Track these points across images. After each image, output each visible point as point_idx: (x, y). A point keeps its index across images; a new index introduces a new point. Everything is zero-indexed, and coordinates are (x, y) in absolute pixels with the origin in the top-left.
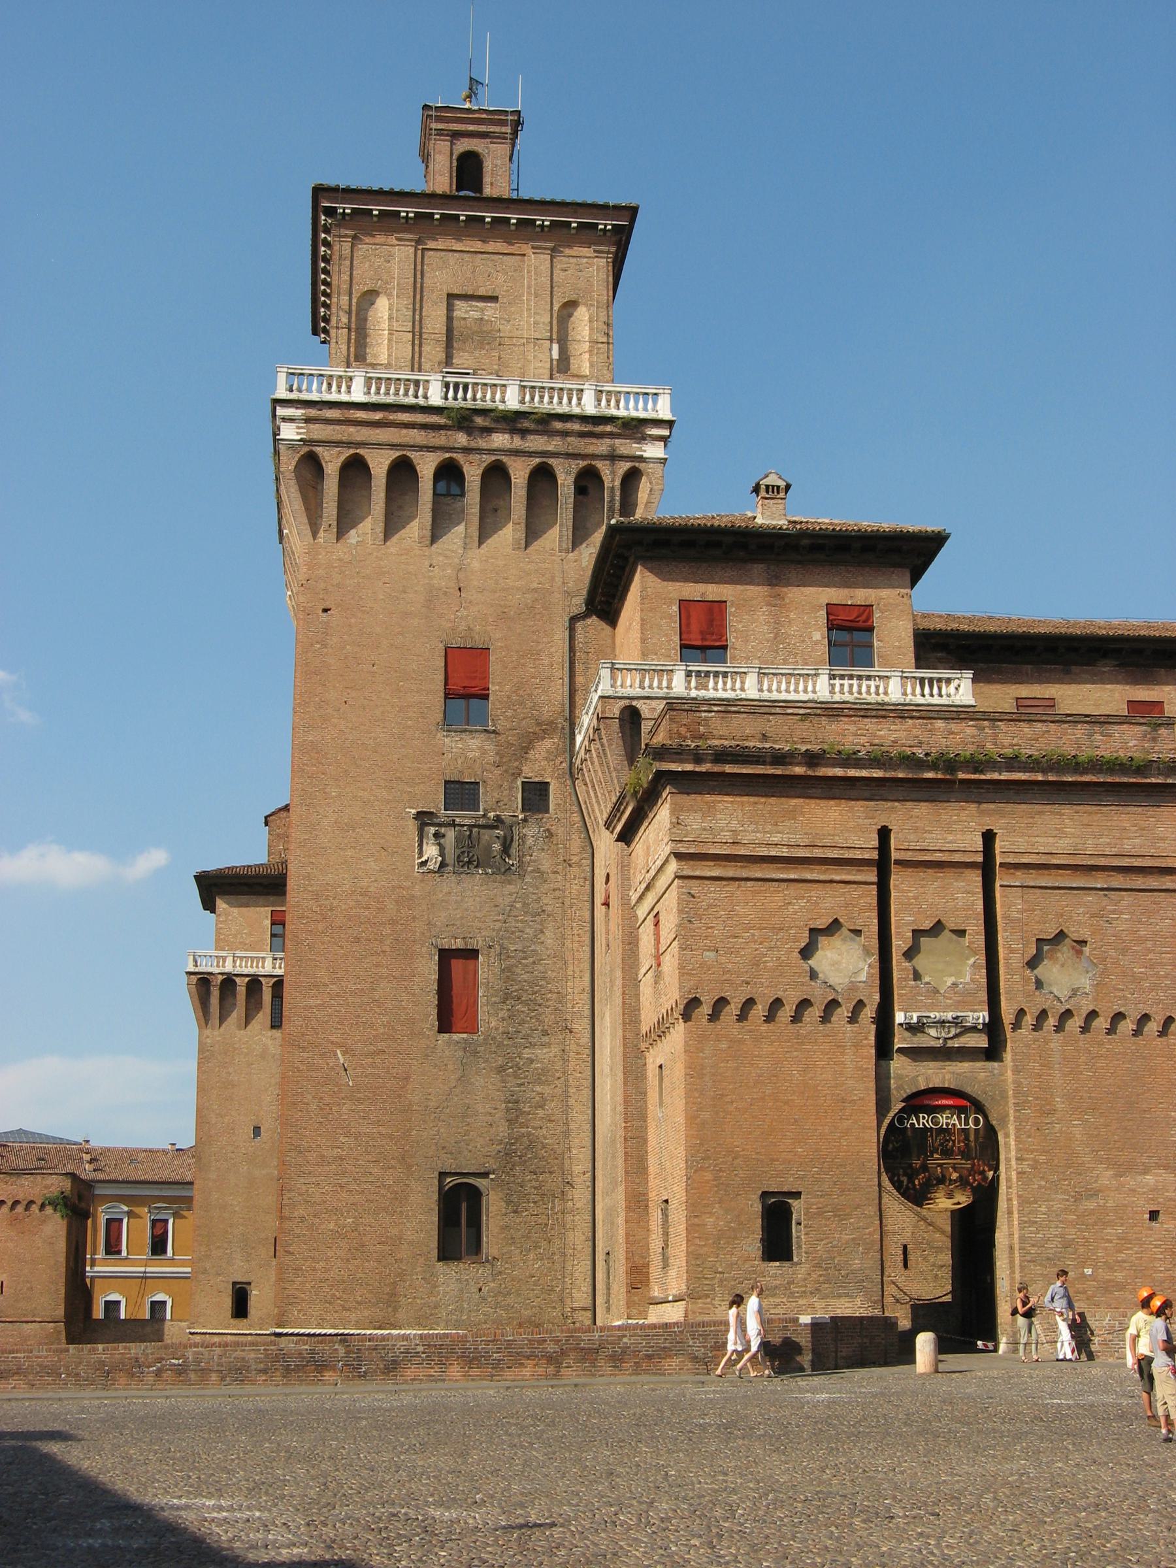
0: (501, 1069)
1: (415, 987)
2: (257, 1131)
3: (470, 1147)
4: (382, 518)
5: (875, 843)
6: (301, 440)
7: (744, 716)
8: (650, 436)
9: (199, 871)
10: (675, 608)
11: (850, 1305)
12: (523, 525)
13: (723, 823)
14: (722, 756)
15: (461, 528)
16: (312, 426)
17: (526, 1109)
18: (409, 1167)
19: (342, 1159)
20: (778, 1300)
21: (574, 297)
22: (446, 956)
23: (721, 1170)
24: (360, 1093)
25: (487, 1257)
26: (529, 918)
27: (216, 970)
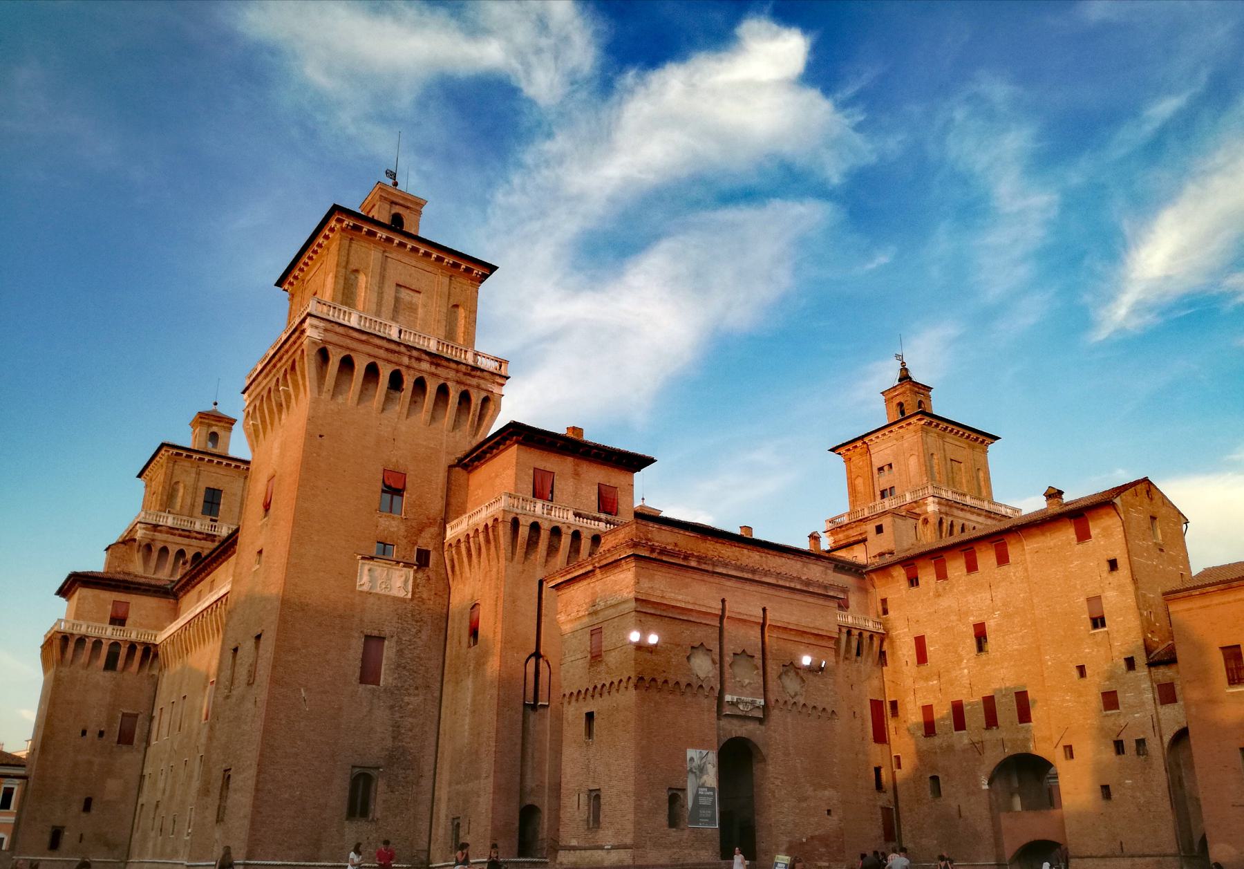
0: (392, 707)
2: (84, 733)
4: (358, 393)
5: (720, 606)
6: (321, 340)
7: (668, 532)
8: (497, 383)
10: (532, 471)
11: (706, 854)
12: (430, 413)
13: (657, 586)
14: (663, 551)
15: (398, 408)
16: (327, 334)
17: (403, 731)
19: (298, 755)
20: (675, 850)
21: (458, 303)
22: (368, 638)
23: (650, 774)
25: (373, 818)
26: (414, 623)
27: (75, 632)
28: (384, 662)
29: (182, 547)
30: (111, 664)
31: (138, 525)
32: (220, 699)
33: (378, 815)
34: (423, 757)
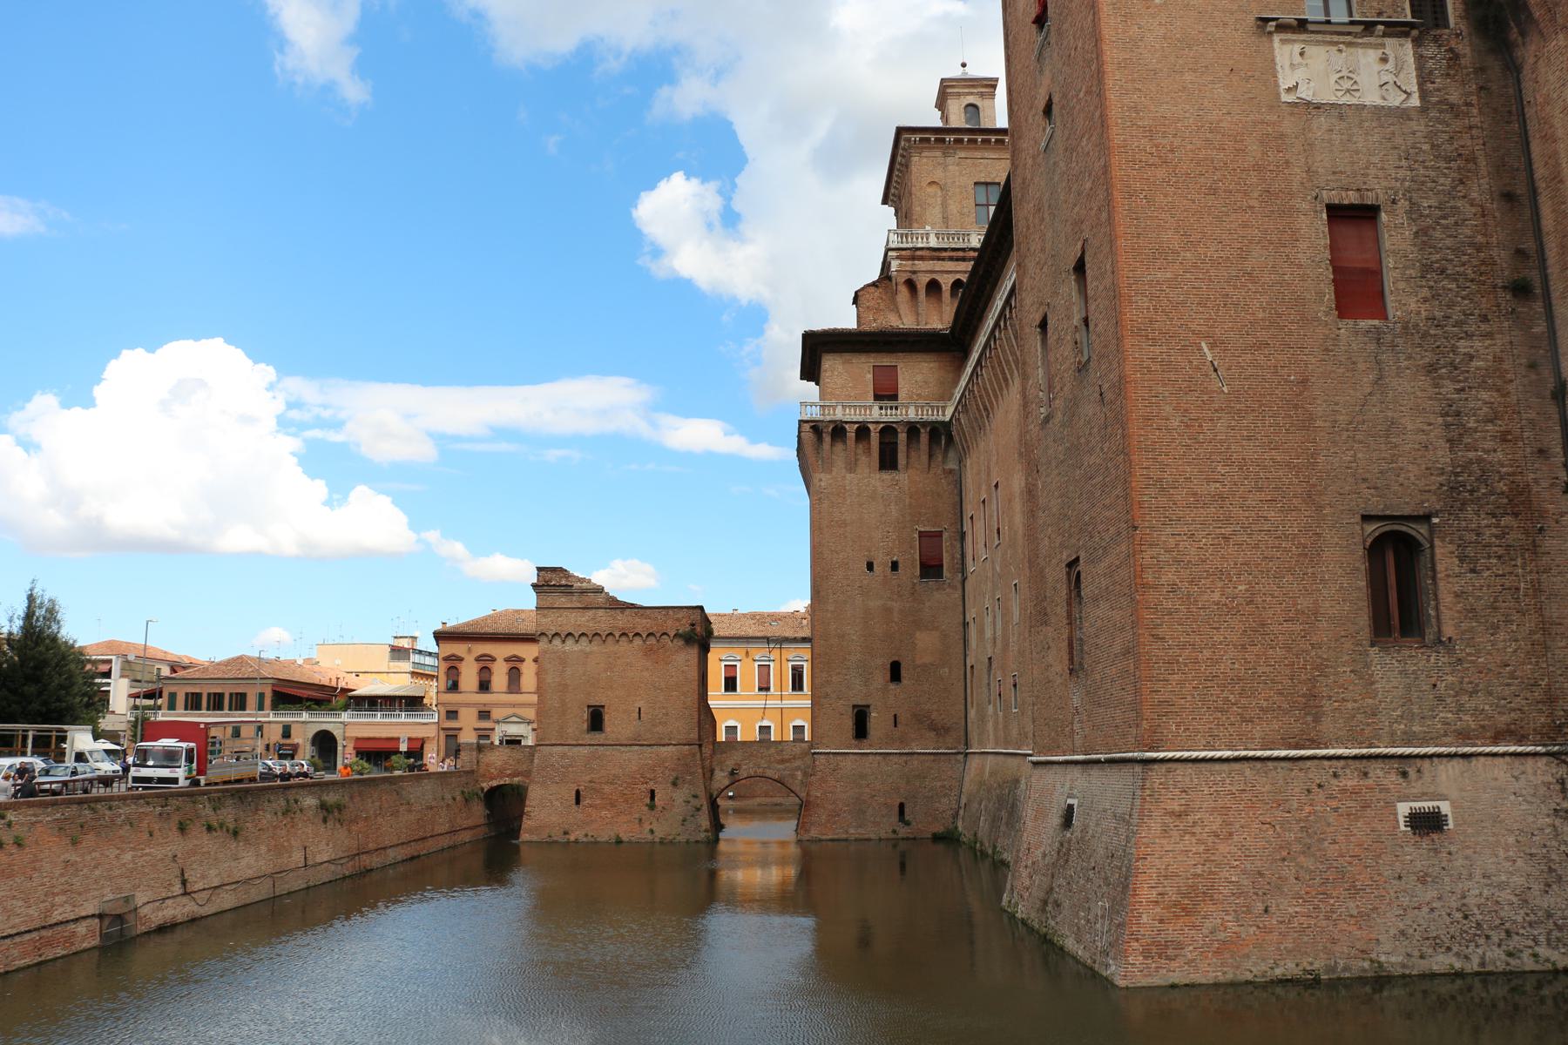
0: (1431, 369)
1: (1299, 256)
2: (870, 566)
3: (1401, 479)
9: (807, 330)
17: (1472, 424)
18: (1320, 508)
19: (1223, 499)
22: (1337, 213)
24: (1239, 402)
26: (1442, 164)
28: (1389, 262)
29: (958, 276)
30: (888, 461)
31: (890, 253)
32: (1034, 428)
33: (1449, 630)
34: (1536, 481)
